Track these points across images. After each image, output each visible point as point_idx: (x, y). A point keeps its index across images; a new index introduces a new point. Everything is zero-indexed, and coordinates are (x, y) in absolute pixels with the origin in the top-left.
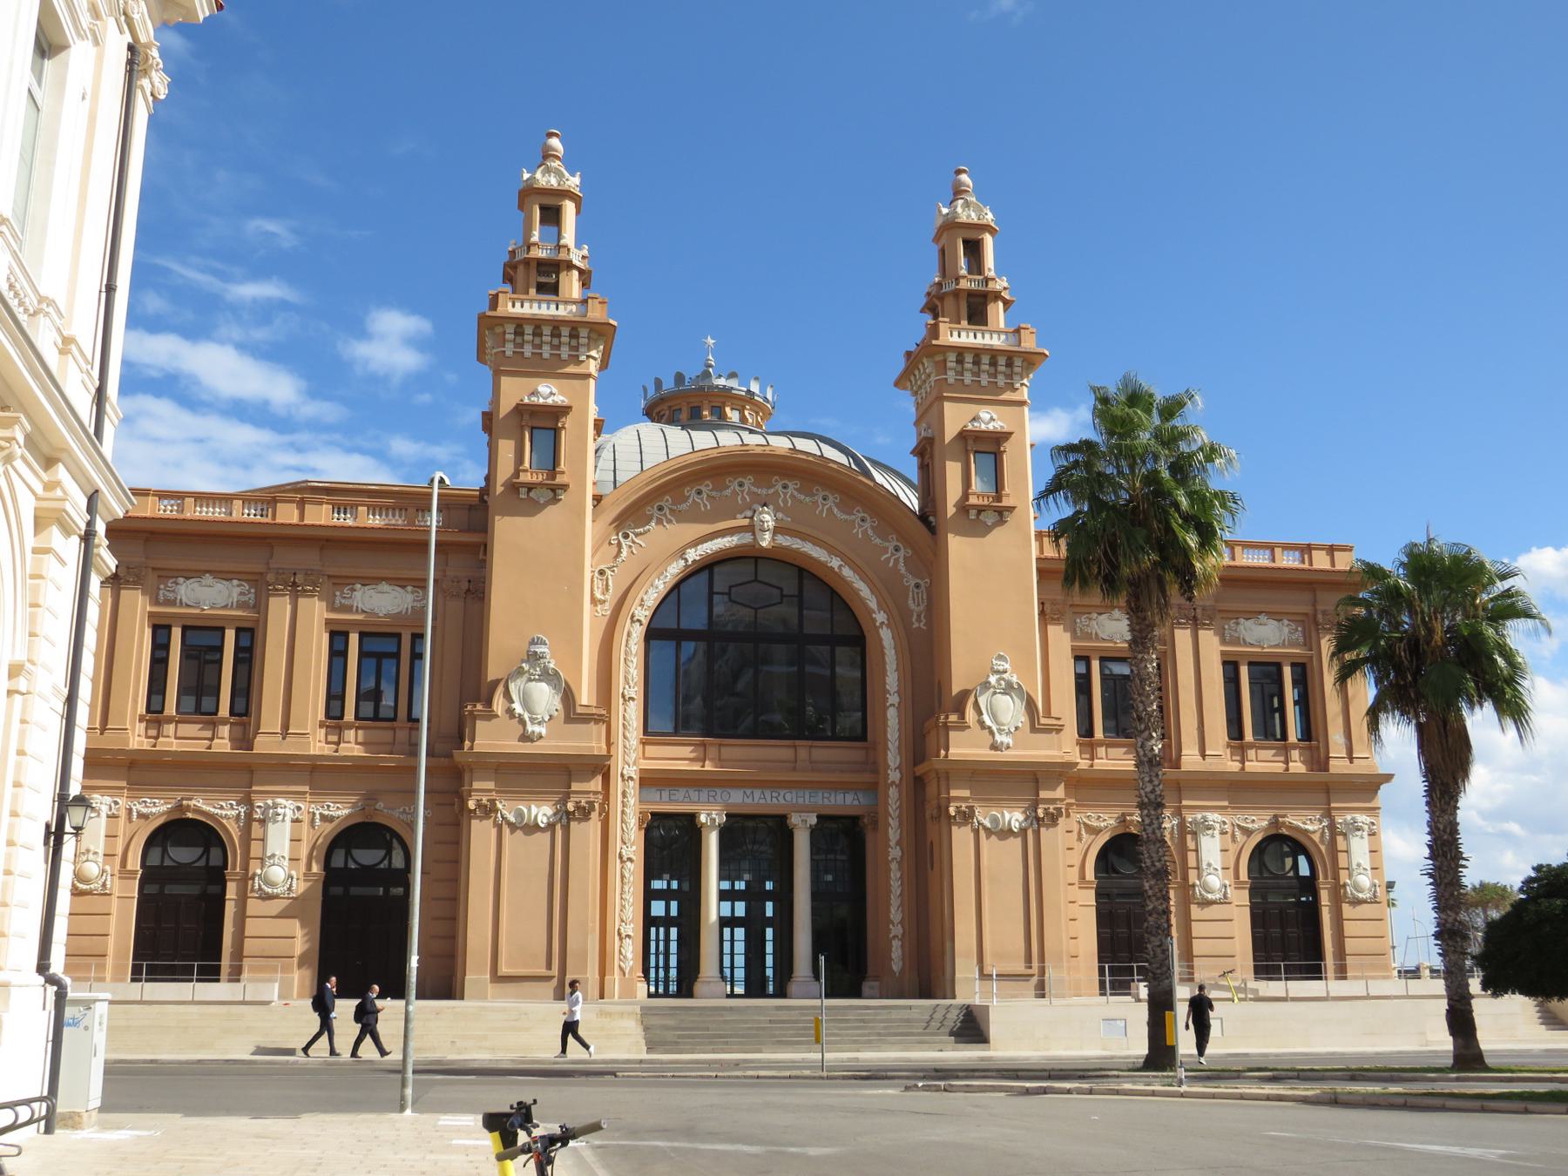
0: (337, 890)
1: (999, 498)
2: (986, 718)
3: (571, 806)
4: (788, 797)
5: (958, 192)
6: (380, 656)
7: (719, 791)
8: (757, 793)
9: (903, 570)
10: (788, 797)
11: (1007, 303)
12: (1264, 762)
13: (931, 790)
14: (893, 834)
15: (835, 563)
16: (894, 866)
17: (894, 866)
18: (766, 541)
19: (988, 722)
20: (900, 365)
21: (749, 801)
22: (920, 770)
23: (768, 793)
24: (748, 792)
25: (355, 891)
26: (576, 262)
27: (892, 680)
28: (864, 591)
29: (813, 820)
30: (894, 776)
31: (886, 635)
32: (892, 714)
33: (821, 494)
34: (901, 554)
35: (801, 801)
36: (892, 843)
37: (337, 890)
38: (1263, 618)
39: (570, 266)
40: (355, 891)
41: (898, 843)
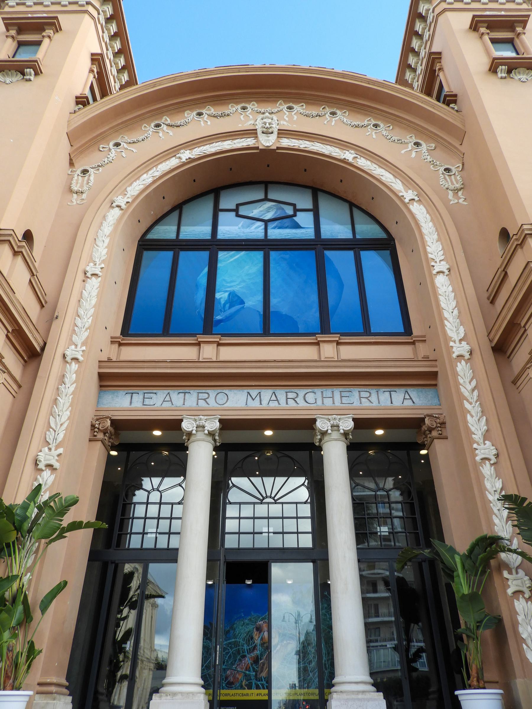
7: (212, 393)
8: (267, 394)
9: (429, 159)
10: (310, 397)
14: (476, 424)
15: (349, 156)
16: (487, 470)
17: (487, 470)
18: (268, 142)
21: (255, 404)
23: (281, 394)
24: (254, 392)
27: (434, 249)
28: (386, 177)
29: (349, 425)
30: (460, 349)
31: (419, 211)
32: (442, 284)
33: (328, 110)
34: (424, 147)
35: (328, 402)
36: (478, 436)
41: (486, 436)
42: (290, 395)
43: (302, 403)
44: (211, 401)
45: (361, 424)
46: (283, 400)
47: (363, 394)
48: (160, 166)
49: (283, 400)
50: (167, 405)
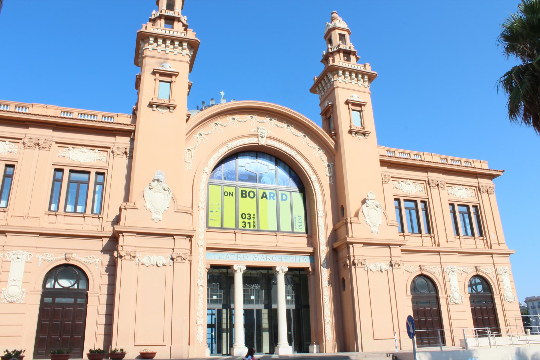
0: (48, 300)
1: (364, 128)
2: (367, 219)
3: (175, 256)
4: (274, 258)
5: (332, 19)
6: (79, 183)
11: (357, 59)
12: (468, 244)
13: (342, 254)
19: (368, 222)
20: (312, 83)
21: (256, 260)
22: (336, 245)
25: (58, 300)
26: (181, 19)
37: (48, 300)
38: (461, 187)
39: (179, 20)
40: (58, 300)
42: (268, 257)
43: (272, 260)
44: (242, 258)
45: (291, 269)
46: (265, 259)
47: (291, 258)
48: (220, 151)
49: (265, 259)
50: (227, 259)
